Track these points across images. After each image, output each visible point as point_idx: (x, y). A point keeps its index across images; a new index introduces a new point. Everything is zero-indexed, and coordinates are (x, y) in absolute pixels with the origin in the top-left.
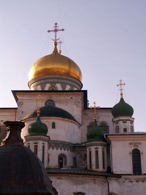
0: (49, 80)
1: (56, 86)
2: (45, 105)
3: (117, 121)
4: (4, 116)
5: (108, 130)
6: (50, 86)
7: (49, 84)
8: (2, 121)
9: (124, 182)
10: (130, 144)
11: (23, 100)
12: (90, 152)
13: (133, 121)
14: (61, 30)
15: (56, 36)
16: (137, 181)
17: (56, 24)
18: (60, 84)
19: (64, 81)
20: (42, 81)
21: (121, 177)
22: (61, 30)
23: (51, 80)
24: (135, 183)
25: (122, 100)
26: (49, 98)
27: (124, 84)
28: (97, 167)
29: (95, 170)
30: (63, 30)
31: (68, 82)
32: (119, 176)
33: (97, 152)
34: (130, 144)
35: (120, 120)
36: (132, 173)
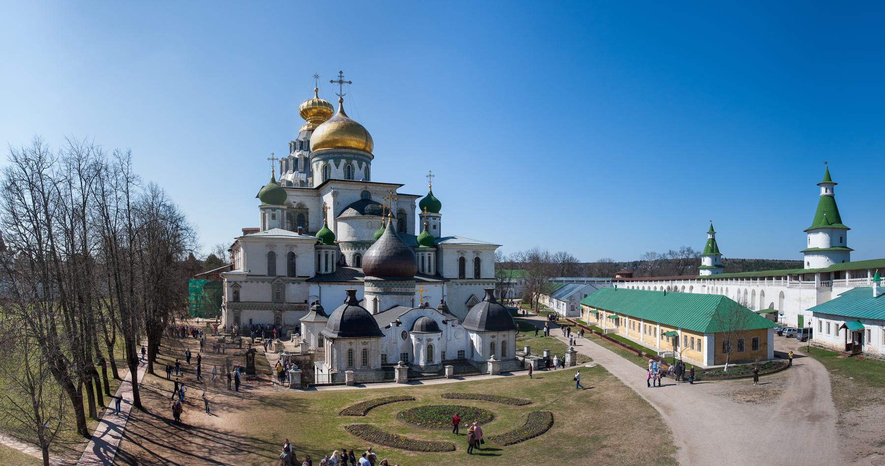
0: (344, 155)
2: (361, 197)
4: (296, 196)
5: (406, 219)
8: (294, 202)
9: (451, 285)
10: (458, 252)
11: (338, 189)
12: (423, 257)
13: (440, 217)
16: (462, 284)
19: (361, 157)
21: (449, 281)
24: (460, 285)
25: (431, 194)
26: (364, 189)
27: (434, 176)
28: (430, 271)
29: (428, 274)
31: (364, 158)
32: (448, 280)
33: (429, 258)
34: (458, 252)
35: (430, 216)
36: (458, 277)
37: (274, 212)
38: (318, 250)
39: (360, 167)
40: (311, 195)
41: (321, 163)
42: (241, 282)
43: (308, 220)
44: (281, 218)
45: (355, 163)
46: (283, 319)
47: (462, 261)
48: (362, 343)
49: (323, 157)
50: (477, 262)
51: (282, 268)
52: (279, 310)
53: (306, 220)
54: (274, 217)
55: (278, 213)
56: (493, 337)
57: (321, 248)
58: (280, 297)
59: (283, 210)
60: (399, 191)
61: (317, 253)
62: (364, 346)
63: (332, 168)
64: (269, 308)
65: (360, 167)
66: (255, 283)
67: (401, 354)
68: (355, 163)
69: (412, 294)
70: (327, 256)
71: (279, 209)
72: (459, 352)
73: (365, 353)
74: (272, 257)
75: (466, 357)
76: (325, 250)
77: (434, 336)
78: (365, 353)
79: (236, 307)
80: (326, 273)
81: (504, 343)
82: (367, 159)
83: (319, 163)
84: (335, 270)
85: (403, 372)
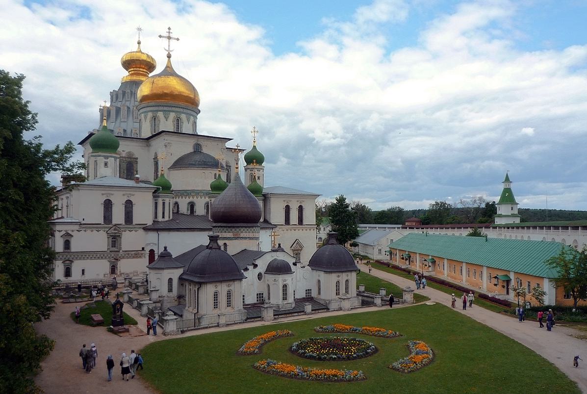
0: (174, 109)
3: (252, 168)
14: (175, 39)
15: (169, 46)
17: (169, 29)
19: (189, 112)
20: (165, 108)
22: (175, 39)
30: (178, 39)
32: (276, 226)
37: (106, 160)
39: (188, 121)
40: (141, 145)
41: (150, 115)
42: (73, 231)
43: (137, 169)
44: (114, 166)
46: (118, 268)
47: (288, 209)
48: (226, 285)
49: (151, 109)
50: (301, 209)
51: (118, 216)
52: (115, 259)
53: (135, 169)
54: (106, 164)
55: (111, 161)
56: (338, 276)
57: (159, 197)
58: (116, 245)
59: (116, 158)
60: (229, 145)
62: (229, 288)
63: (161, 120)
64: (104, 258)
65: (188, 121)
66: (89, 231)
67: (257, 294)
68: (183, 116)
69: (257, 238)
70: (164, 204)
71: (111, 157)
72: (306, 290)
73: (229, 295)
74: (108, 205)
75: (312, 296)
77: (288, 279)
78: (229, 295)
79: (67, 259)
80: (163, 220)
81: (347, 281)
82: (195, 114)
84: (171, 218)
85: (270, 311)
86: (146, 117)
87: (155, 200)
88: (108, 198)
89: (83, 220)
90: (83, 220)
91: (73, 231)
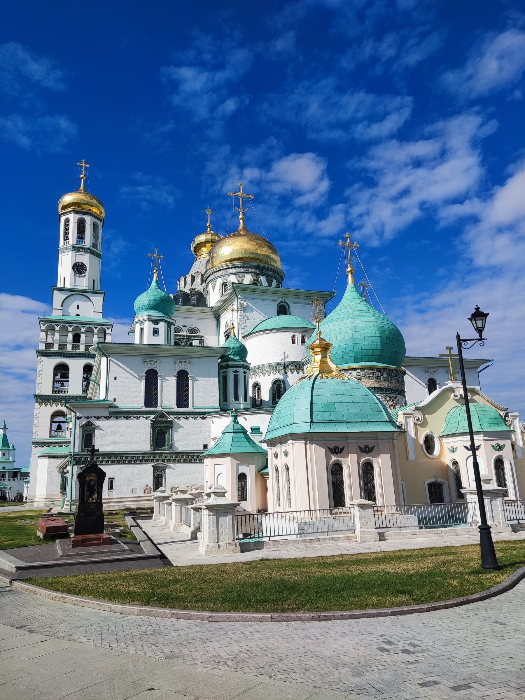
0: (250, 270)
1: (260, 279)
6: (252, 278)
7: (251, 275)
8: (184, 326)
18: (265, 277)
20: (238, 270)
23: (253, 270)
31: (274, 274)
37: (156, 326)
38: (223, 370)
41: (219, 282)
45: (263, 279)
49: (220, 273)
54: (155, 332)
57: (228, 367)
59: (169, 324)
61: (222, 375)
70: (236, 377)
76: (234, 369)
83: (216, 282)
86: (214, 288)
87: (223, 373)
88: (152, 367)
89: (115, 400)
90: (115, 400)
91: (98, 418)
